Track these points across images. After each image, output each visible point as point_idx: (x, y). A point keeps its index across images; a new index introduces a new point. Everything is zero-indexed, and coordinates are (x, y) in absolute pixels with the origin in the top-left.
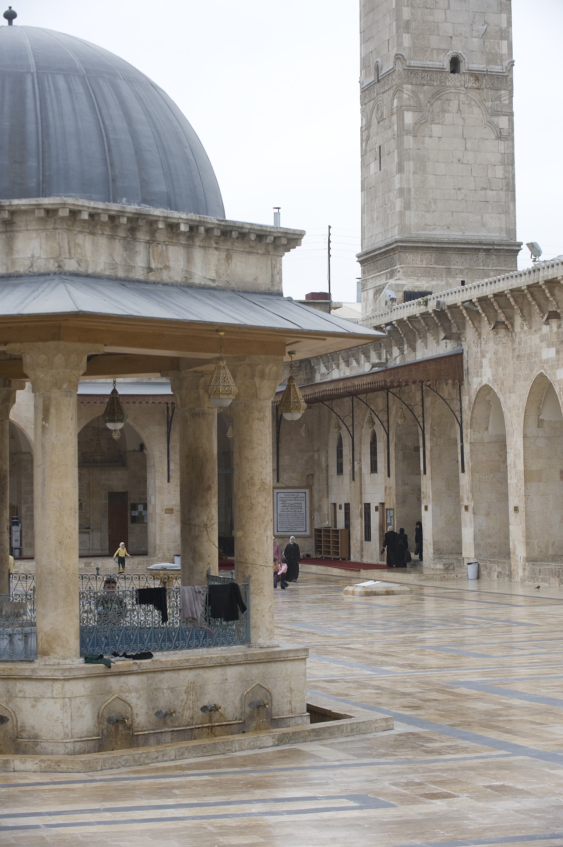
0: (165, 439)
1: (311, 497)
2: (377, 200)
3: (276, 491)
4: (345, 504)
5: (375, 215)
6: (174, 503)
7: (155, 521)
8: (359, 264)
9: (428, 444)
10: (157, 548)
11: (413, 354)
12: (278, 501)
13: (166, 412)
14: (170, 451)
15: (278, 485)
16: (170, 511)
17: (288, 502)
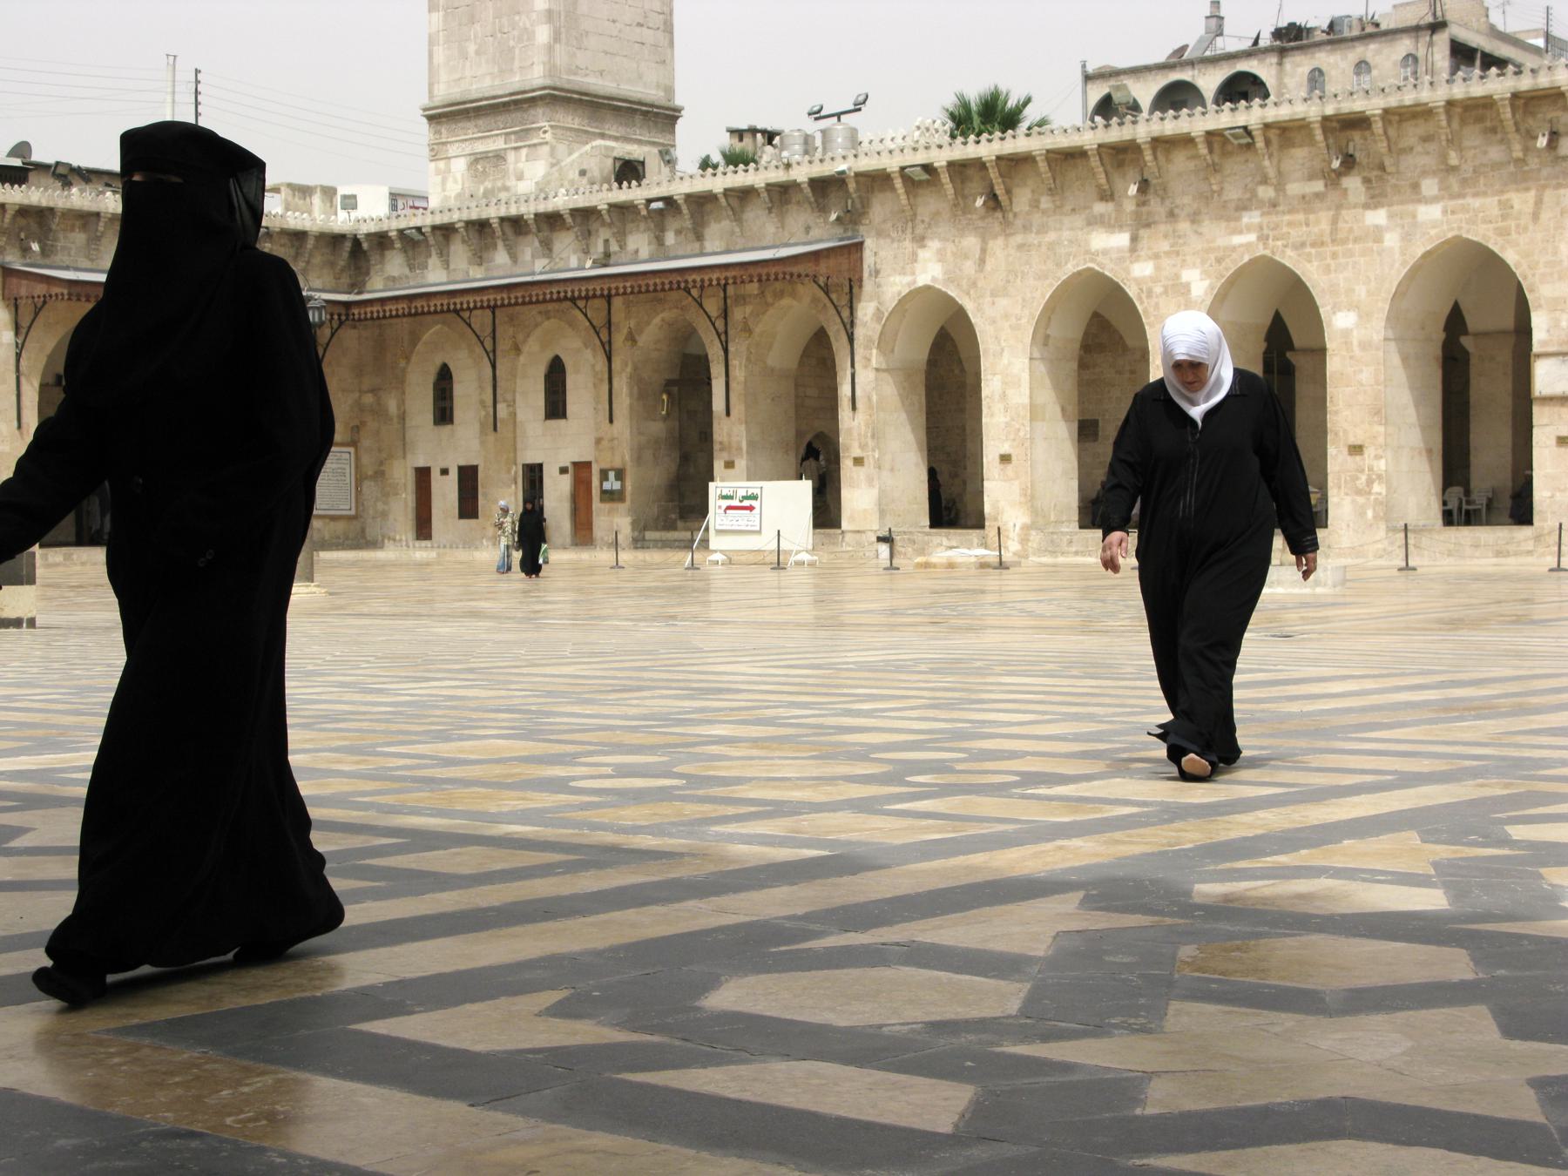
1: (357, 459)
2: (477, 27)
4: (462, 469)
5: (472, 48)
8: (425, 120)
9: (738, 373)
11: (697, 245)
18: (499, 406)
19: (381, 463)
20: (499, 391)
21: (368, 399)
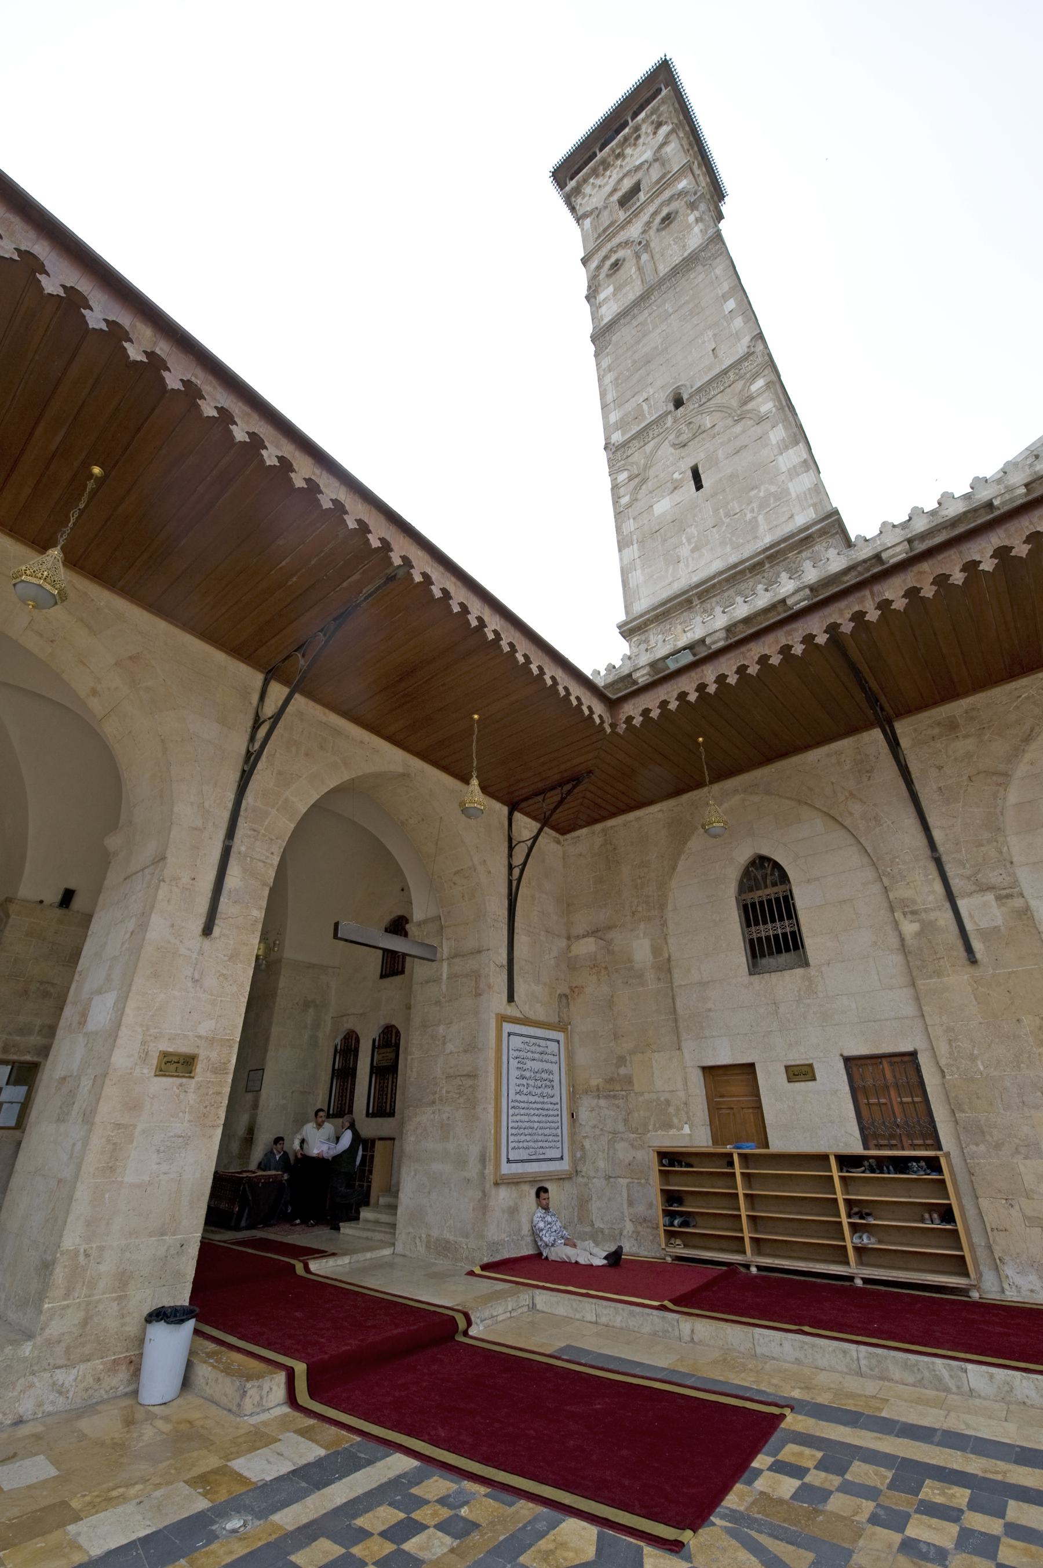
0: (232, 777)
1: (570, 1057)
3: (507, 1027)
6: (206, 1027)
7: (88, 1118)
10: (59, 1274)
12: (511, 1060)
13: (255, 698)
14: (241, 821)
15: (511, 1011)
16: (177, 1064)
17: (529, 1064)
18: (962, 904)
19: (622, 1060)
20: (951, 871)
21: (586, 947)
